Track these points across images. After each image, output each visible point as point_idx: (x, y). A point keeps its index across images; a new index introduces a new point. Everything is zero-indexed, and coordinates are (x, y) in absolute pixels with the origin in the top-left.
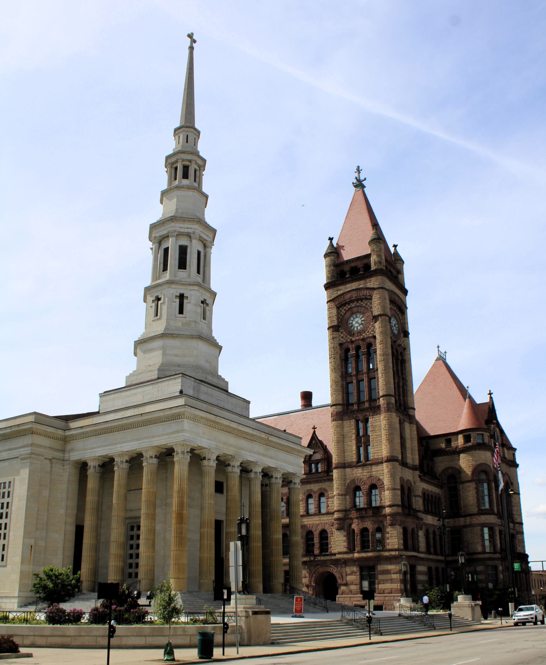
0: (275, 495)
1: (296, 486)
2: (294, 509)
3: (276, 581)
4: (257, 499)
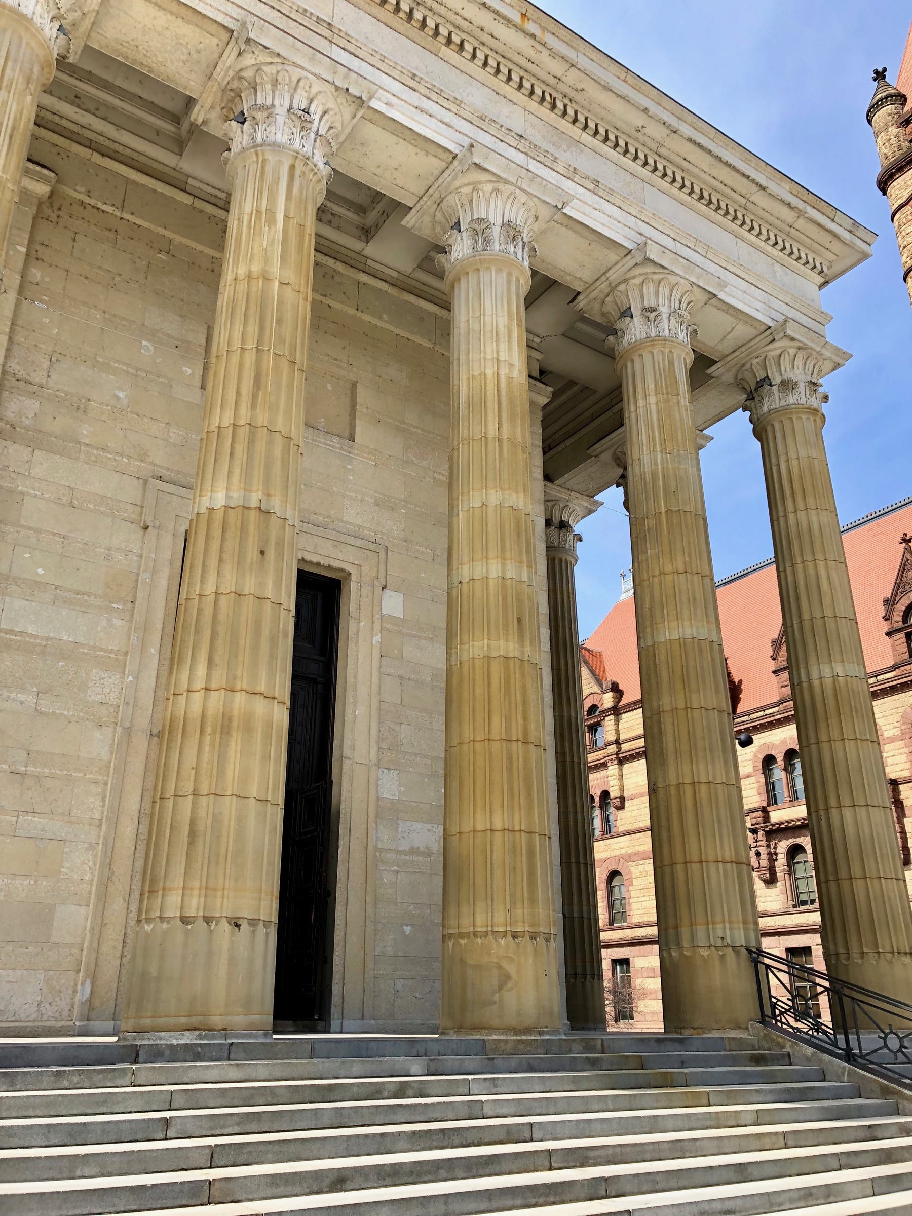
0: (652, 400)
1: (791, 399)
2: (802, 515)
3: (700, 931)
4: (489, 372)
